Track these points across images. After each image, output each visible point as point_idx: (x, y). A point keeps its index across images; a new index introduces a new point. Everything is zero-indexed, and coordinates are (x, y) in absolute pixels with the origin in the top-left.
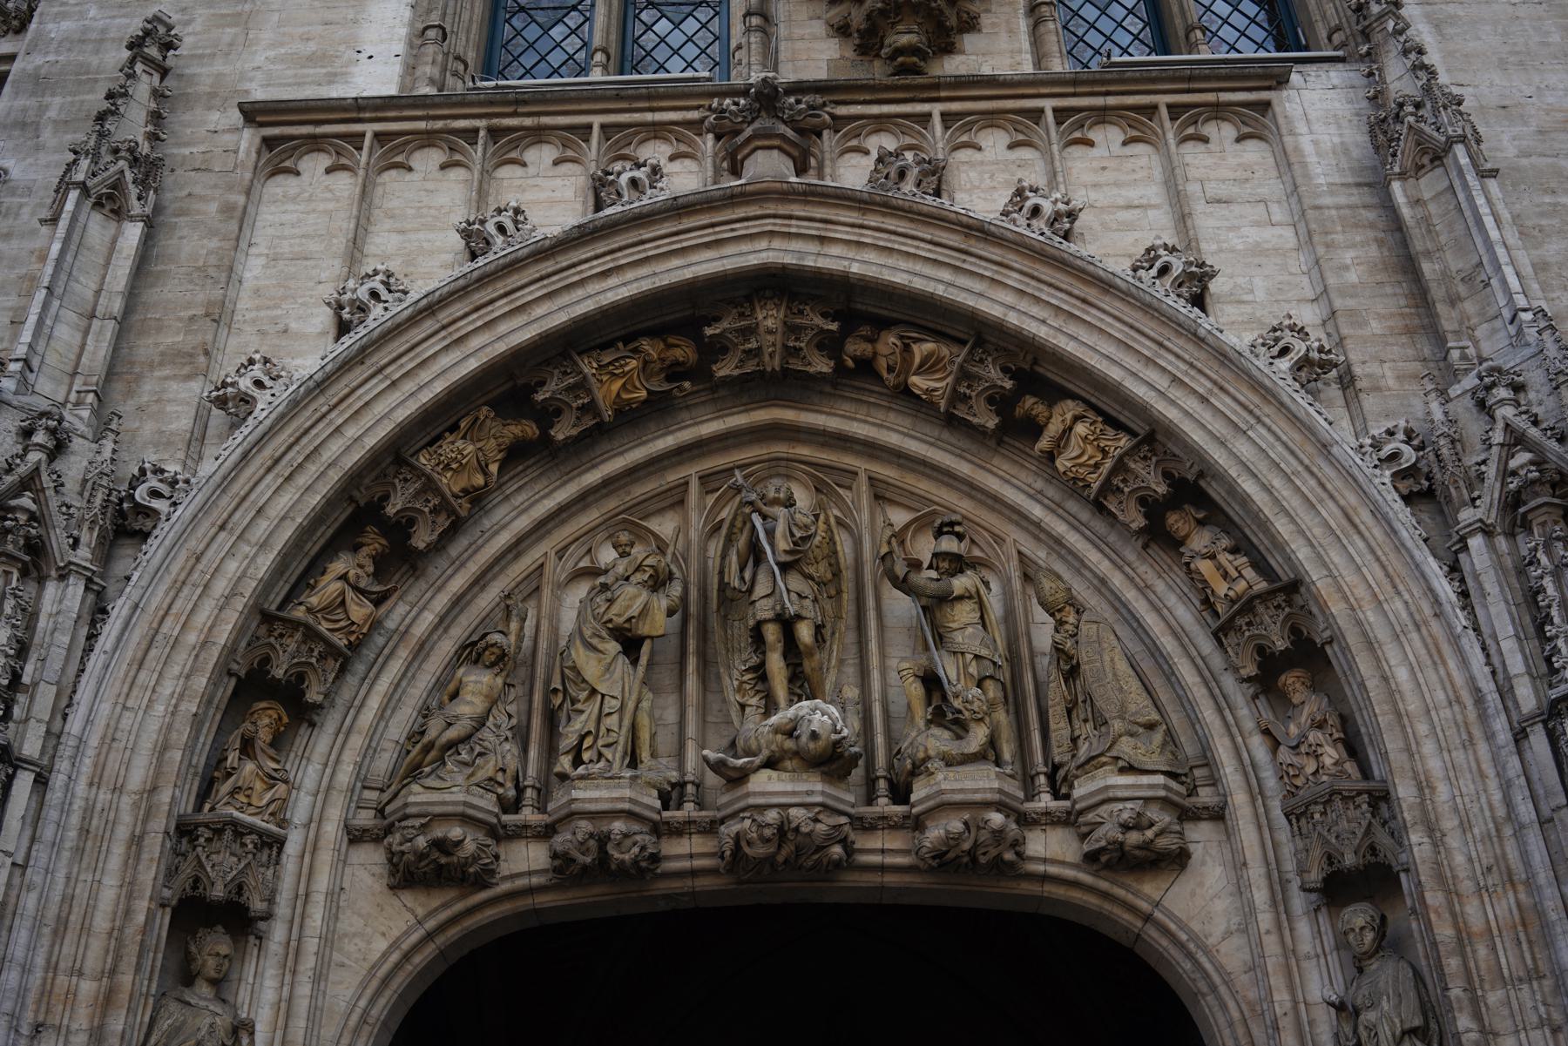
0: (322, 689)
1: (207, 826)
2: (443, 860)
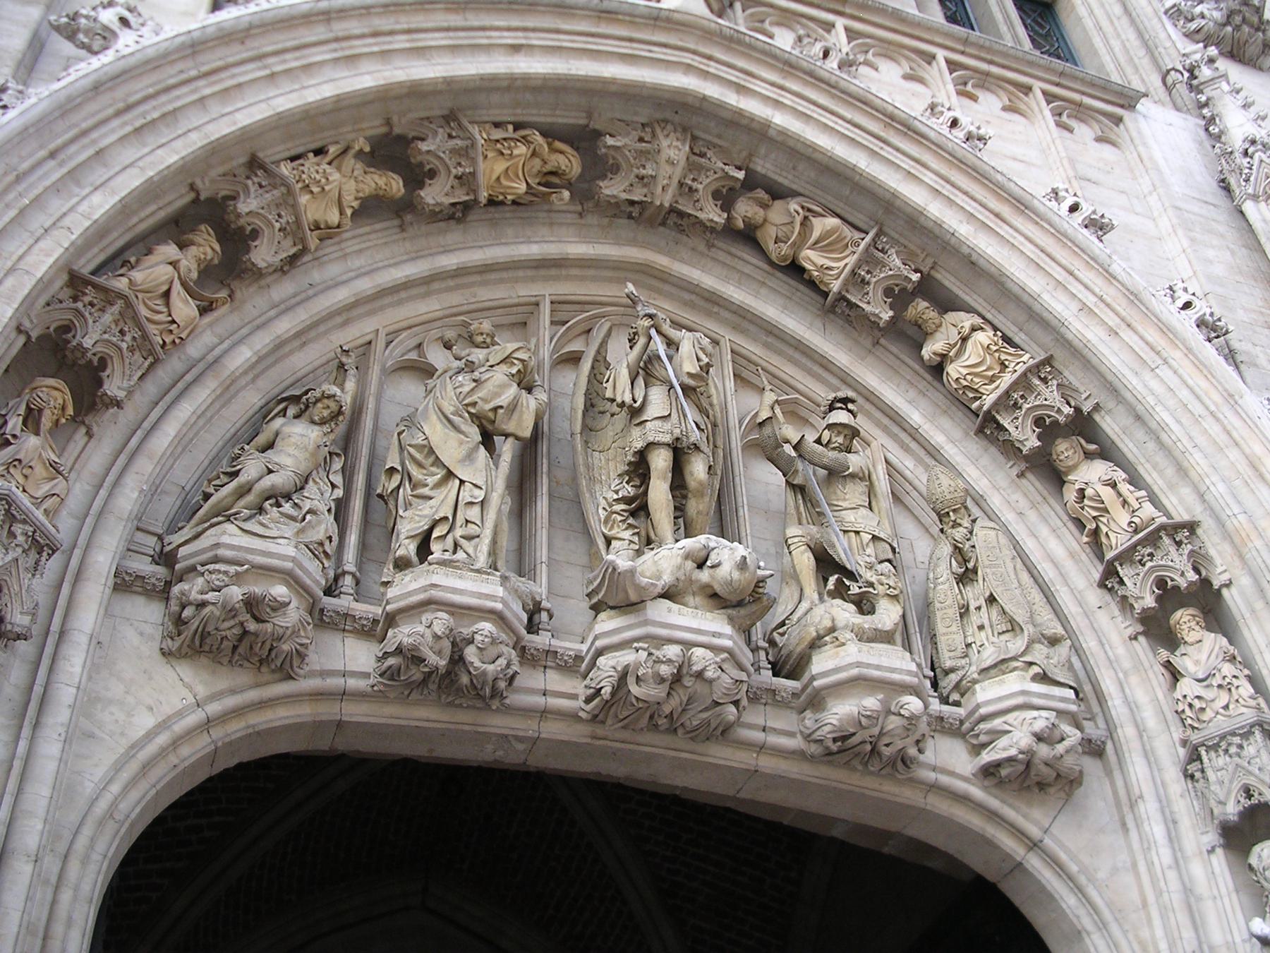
0: (125, 384)
2: (252, 626)
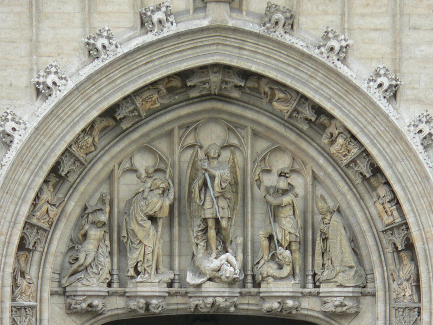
1: (15, 307)
2: (90, 309)
